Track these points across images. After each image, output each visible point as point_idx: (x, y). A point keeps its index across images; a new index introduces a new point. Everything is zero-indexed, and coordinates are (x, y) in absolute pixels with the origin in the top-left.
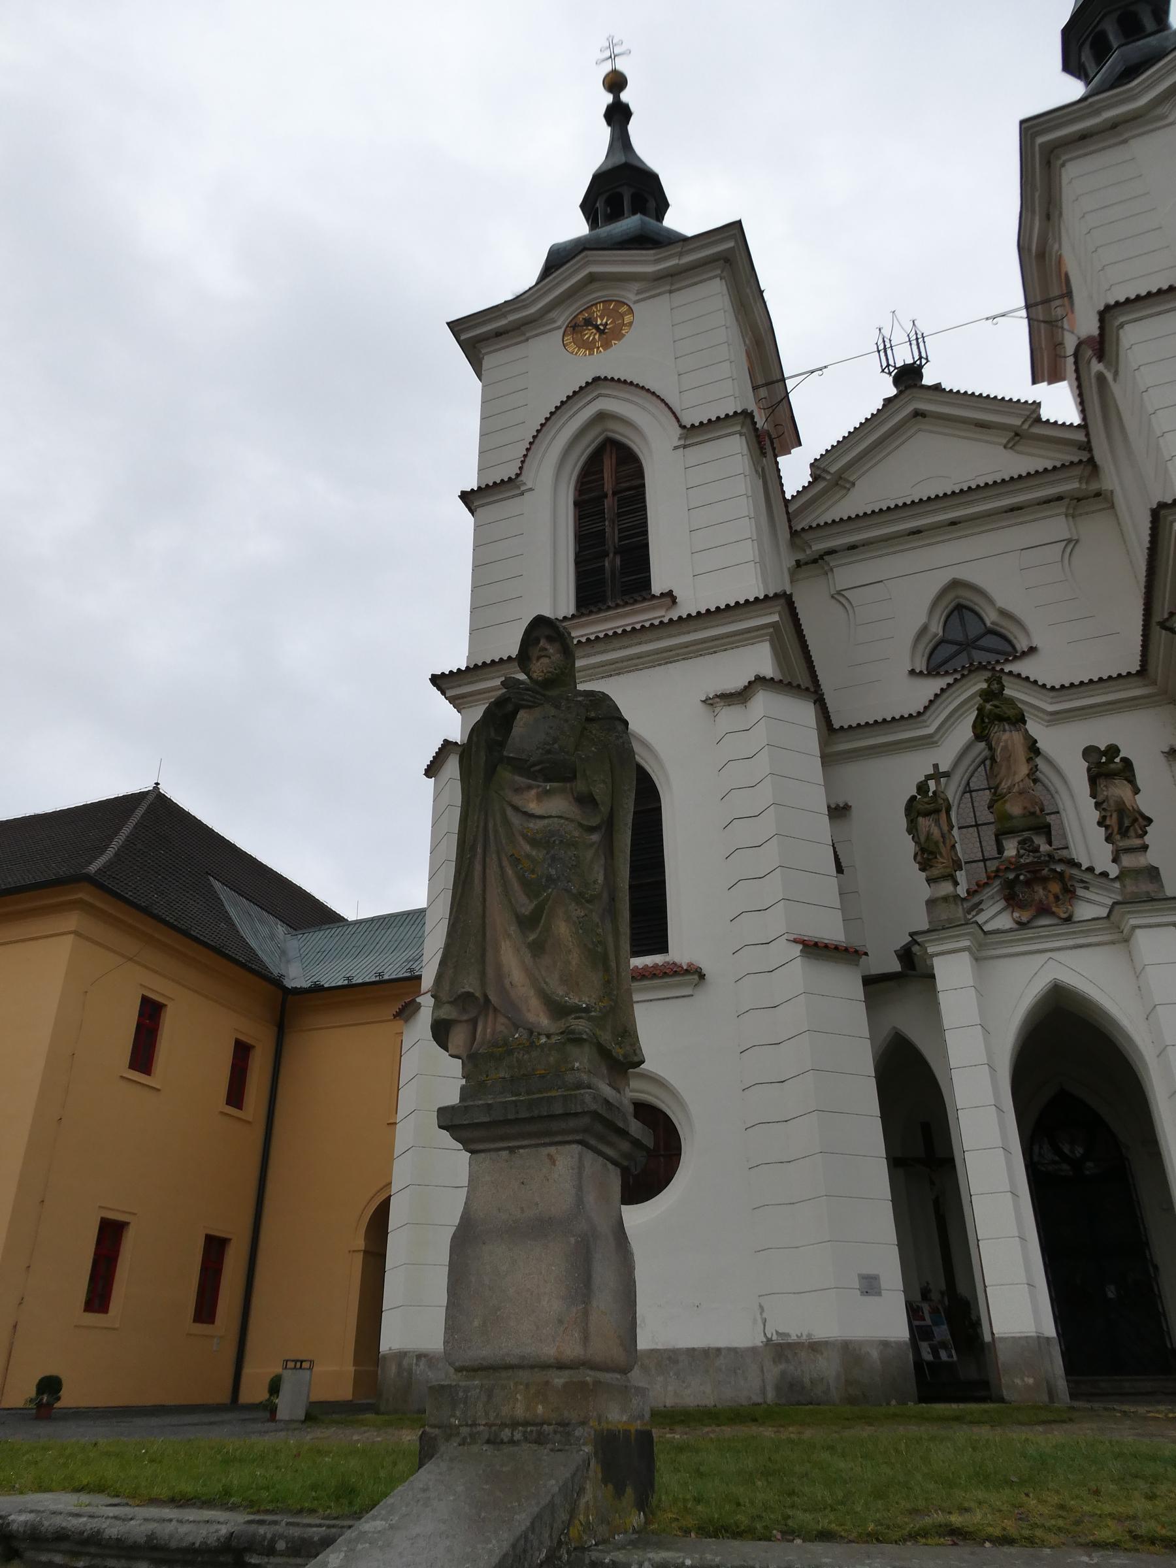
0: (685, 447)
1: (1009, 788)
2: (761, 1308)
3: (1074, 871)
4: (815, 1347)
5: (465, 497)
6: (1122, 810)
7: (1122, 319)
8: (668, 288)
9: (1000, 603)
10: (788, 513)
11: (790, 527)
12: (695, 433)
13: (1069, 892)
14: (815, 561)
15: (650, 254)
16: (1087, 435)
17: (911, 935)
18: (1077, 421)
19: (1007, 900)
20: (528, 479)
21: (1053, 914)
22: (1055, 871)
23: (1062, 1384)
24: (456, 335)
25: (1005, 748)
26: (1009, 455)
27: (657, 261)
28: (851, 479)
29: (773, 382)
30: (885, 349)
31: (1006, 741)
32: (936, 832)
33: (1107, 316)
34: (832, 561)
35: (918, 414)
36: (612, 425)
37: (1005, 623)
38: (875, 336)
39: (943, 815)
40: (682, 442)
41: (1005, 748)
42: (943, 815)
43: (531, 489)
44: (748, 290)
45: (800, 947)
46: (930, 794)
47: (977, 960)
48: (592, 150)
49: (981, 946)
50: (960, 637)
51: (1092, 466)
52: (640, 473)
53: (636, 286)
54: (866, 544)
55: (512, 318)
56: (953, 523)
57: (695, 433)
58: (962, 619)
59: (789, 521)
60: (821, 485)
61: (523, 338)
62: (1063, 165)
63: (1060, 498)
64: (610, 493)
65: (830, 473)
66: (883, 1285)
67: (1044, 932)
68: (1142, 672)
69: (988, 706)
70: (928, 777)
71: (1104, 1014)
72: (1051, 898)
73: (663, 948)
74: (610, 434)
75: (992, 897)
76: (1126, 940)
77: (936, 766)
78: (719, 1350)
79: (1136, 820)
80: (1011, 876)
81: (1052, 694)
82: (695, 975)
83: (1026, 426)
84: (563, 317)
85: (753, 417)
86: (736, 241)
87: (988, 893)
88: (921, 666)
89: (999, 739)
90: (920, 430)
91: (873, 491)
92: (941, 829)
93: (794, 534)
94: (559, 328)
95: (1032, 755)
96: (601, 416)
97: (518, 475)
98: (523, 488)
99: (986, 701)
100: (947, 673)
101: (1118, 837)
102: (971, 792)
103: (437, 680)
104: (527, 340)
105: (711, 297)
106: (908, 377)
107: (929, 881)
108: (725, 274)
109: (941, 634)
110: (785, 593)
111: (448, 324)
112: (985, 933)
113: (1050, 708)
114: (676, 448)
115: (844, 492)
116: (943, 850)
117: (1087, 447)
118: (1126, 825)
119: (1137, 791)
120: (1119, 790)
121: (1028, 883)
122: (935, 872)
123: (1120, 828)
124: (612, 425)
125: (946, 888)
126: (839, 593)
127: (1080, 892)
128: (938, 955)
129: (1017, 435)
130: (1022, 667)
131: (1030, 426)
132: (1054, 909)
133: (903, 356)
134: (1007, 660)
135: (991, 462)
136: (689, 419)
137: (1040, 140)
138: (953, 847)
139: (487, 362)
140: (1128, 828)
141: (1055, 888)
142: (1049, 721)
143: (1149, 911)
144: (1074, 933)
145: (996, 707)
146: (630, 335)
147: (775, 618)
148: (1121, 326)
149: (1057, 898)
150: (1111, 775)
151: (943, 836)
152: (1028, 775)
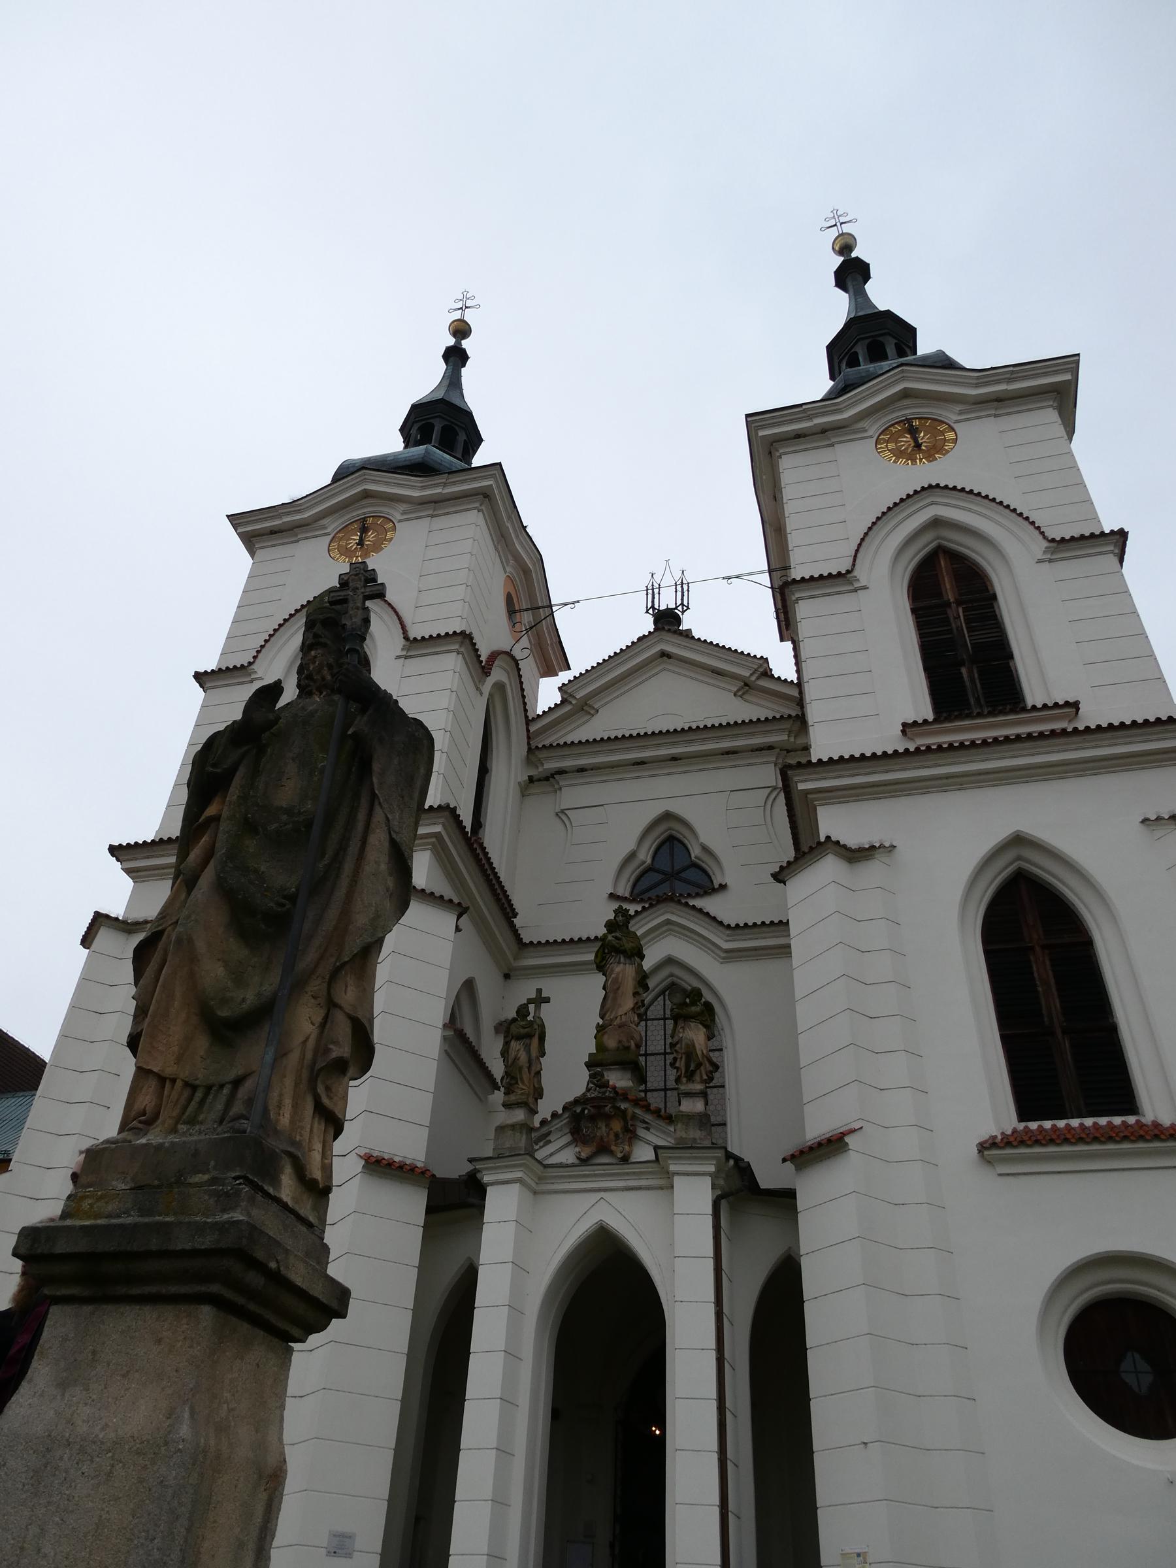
0: (406, 657)
1: (611, 1020)
5: (198, 676)
6: (690, 1053)
7: (797, 595)
8: (430, 512)
9: (703, 839)
10: (528, 731)
11: (529, 744)
12: (416, 645)
13: (631, 1135)
14: (547, 779)
15: (417, 481)
16: (801, 693)
17: (471, 1160)
18: (792, 676)
19: (572, 1134)
21: (612, 1153)
22: (619, 1108)
24: (235, 527)
25: (616, 980)
26: (738, 702)
27: (423, 488)
29: (531, 609)
30: (652, 591)
31: (618, 974)
32: (523, 1056)
33: (787, 591)
34: (562, 780)
35: (664, 654)
37: (705, 858)
39: (535, 1042)
40: (404, 653)
41: (616, 980)
42: (535, 1042)
44: (509, 525)
45: (363, 1162)
46: (530, 1018)
47: (535, 1193)
48: (426, 380)
49: (541, 1179)
50: (668, 869)
53: (403, 507)
54: (595, 768)
55: (285, 519)
56: (674, 759)
59: (529, 738)
60: (567, 708)
63: (770, 748)
65: (579, 700)
66: (357, 1546)
67: (599, 1170)
69: (610, 937)
70: (530, 1001)
72: (612, 1137)
75: (560, 1129)
77: (539, 991)
79: (699, 1065)
80: (578, 1110)
81: (728, 932)
83: (753, 678)
84: (333, 525)
85: (472, 639)
86: (496, 481)
87: (557, 1124)
89: (612, 971)
90: (664, 669)
91: (610, 721)
92: (529, 1052)
93: (530, 750)
94: (329, 534)
95: (641, 990)
97: (250, 664)
99: (610, 932)
100: (642, 901)
101: (684, 1080)
102: (646, 1020)
104: (298, 541)
105: (468, 529)
106: (667, 620)
108: (483, 508)
109: (649, 861)
110: (448, 805)
112: (546, 1166)
113: (725, 946)
114: (398, 657)
115: (588, 717)
116: (526, 1076)
122: (513, 1098)
123: (686, 1071)
125: (519, 1115)
126: (563, 811)
127: (641, 1132)
128: (492, 1184)
129: (746, 685)
130: (708, 904)
131: (758, 678)
132: (613, 1148)
133: (667, 601)
134: (698, 895)
135: (717, 705)
136: (415, 632)
137: (761, 433)
138: (538, 1073)
139: (259, 553)
140: (693, 1072)
141: (617, 1126)
142: (724, 958)
143: (689, 1158)
144: (628, 1174)
145: (616, 938)
146: (388, 549)
147: (438, 829)
148: (797, 599)
149: (617, 1135)
150: (688, 1018)
151: (530, 1061)
152: (633, 1009)
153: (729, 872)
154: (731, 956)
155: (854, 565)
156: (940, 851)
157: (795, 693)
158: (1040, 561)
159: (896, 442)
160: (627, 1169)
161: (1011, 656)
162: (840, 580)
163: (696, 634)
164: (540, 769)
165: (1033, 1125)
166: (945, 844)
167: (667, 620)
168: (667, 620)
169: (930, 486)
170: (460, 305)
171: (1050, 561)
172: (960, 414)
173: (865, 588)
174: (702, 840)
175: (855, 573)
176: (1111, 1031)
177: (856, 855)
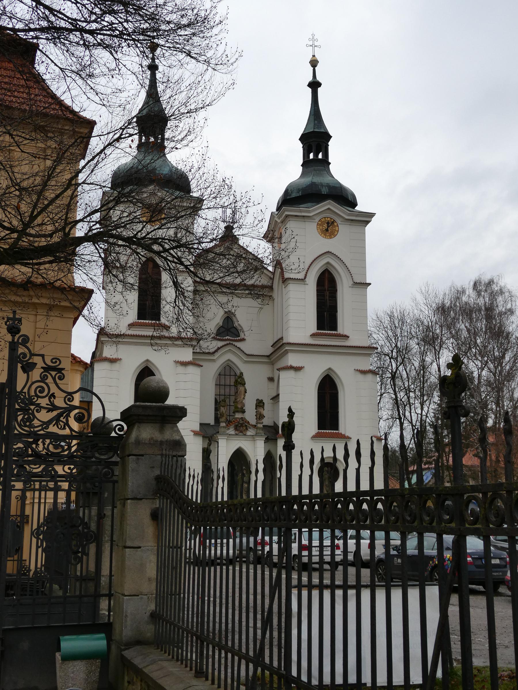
13: (247, 429)
32: (224, 411)
51: (271, 288)
58: (228, 321)
71: (246, 453)
117: (272, 279)
118: (260, 417)
120: (261, 410)
141: (245, 428)
150: (260, 406)
154: (246, 362)
155: (306, 275)
157: (272, 276)
162: (303, 280)
165: (320, 431)
166: (315, 368)
168: (229, 229)
169: (329, 252)
172: (342, 221)
175: (306, 280)
176: (337, 413)
177: (298, 369)
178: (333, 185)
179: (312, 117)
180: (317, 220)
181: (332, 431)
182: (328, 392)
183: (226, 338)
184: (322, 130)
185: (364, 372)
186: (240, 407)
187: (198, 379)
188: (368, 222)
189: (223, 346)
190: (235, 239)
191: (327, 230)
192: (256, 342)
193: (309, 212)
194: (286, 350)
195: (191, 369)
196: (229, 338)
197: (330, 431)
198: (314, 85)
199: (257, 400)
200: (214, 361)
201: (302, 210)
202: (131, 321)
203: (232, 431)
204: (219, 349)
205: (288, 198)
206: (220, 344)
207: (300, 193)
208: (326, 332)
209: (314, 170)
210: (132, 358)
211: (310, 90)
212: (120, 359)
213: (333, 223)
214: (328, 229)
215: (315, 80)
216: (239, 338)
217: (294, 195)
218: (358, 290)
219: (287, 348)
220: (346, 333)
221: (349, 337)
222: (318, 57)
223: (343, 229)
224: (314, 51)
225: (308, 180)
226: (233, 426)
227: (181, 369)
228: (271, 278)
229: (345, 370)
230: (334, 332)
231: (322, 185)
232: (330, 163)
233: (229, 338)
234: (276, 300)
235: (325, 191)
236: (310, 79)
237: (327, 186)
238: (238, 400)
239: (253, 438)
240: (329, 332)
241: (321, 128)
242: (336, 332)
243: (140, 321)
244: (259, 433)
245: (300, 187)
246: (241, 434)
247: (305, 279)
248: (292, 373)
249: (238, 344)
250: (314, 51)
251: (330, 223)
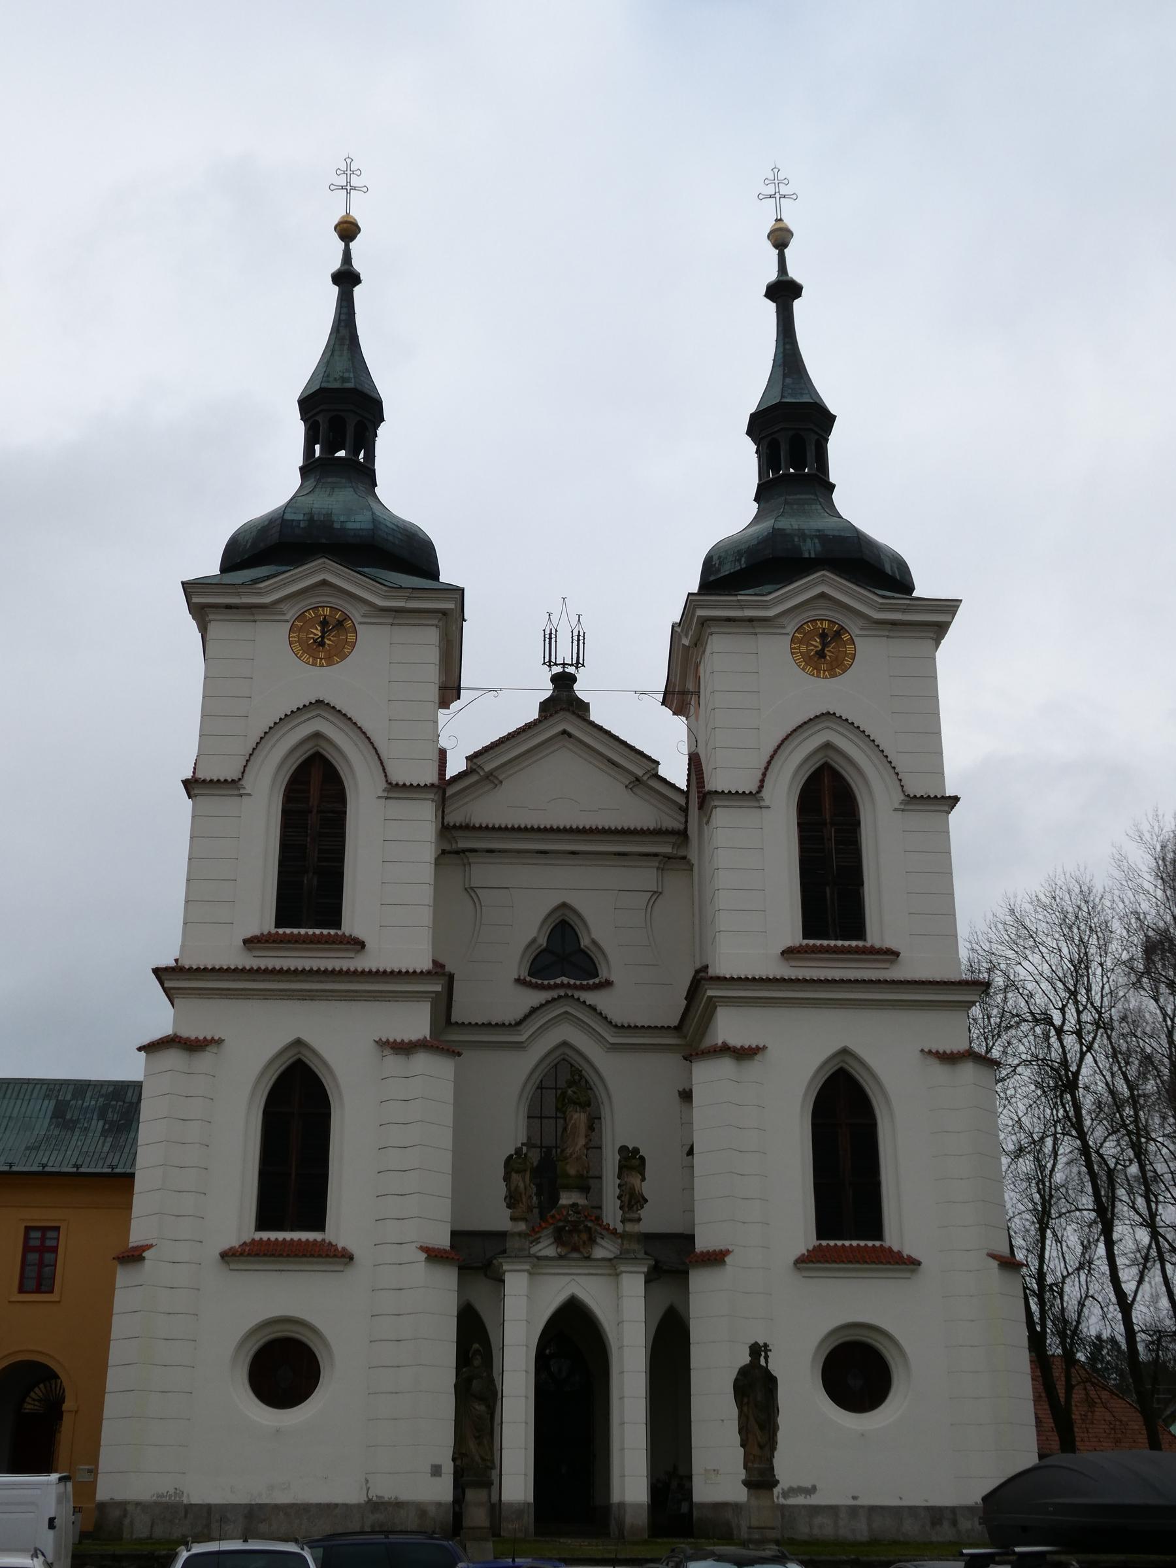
0: (386, 798)
2: (367, 1481)
3: (598, 1228)
4: (399, 1505)
8: (390, 621)
12: (396, 790)
13: (592, 1241)
14: (457, 852)
20: (248, 783)
23: (532, 1528)
27: (387, 597)
28: (501, 778)
30: (550, 638)
32: (521, 1185)
34: (472, 858)
35: (564, 732)
36: (324, 744)
37: (593, 948)
38: (542, 623)
43: (249, 795)
51: (682, 835)
52: (341, 797)
53: (365, 609)
54: (500, 851)
56: (573, 853)
57: (396, 790)
61: (251, 618)
62: (711, 634)
63: (656, 855)
64: (315, 810)
67: (572, 1263)
68: (678, 1028)
73: (320, 1226)
74: (321, 750)
76: (617, 1275)
78: (336, 1505)
80: (561, 1224)
82: (347, 1257)
88: (524, 974)
94: (287, 621)
96: (317, 735)
98: (242, 791)
103: (157, 972)
104: (255, 621)
107: (513, 1219)
111: (183, 583)
113: (612, 1040)
114: (379, 797)
115: (492, 786)
117: (685, 810)
118: (632, 1201)
119: (643, 1179)
120: (635, 1180)
121: (570, 1231)
124: (324, 744)
126: (472, 888)
127: (599, 1240)
133: (564, 652)
139: (214, 629)
141: (585, 1236)
147: (439, 988)
148: (716, 807)
149: (584, 1243)
150: (632, 1168)
153: (615, 966)
154: (615, 1048)
156: (797, 1049)
157: (682, 802)
158: (896, 810)
159: (808, 645)
160: (589, 1263)
161: (862, 884)
162: (752, 798)
163: (594, 716)
164: (454, 846)
165: (824, 1243)
167: (564, 681)
168: (564, 681)
169: (828, 715)
170: (342, 181)
171: (903, 810)
173: (768, 807)
174: (593, 936)
175: (763, 794)
176: (877, 1185)
178: (837, 533)
179: (780, 371)
180: (791, 628)
181: (862, 1243)
182: (844, 1120)
183: (558, 981)
184: (806, 399)
185: (949, 1059)
186: (572, 1171)
187: (447, 1091)
188: (939, 630)
189: (548, 1002)
190: (580, 709)
191: (821, 654)
192: (638, 990)
193: (765, 606)
194: (711, 998)
195: (422, 1062)
196: (565, 980)
197: (855, 1243)
198: (784, 292)
199: (623, 1149)
200: (519, 1046)
201: (745, 604)
202: (253, 930)
203: (546, 1248)
204: (533, 1011)
205: (712, 578)
206: (537, 998)
207: (743, 560)
208: (832, 943)
209: (786, 503)
210: (254, 1039)
211: (772, 306)
212: (218, 1042)
213: (838, 634)
214: (825, 651)
215: (784, 278)
216: (597, 980)
217: (726, 570)
218: (919, 819)
219: (710, 993)
220: (890, 943)
221: (897, 954)
222: (790, 222)
223: (870, 651)
224: (778, 208)
225: (767, 525)
226: (545, 1232)
227: (393, 1063)
228: (681, 808)
229: (890, 1052)
230: (854, 943)
231: (803, 535)
232: (833, 487)
233: (565, 980)
234: (696, 868)
235: (810, 549)
236: (772, 275)
237: (816, 536)
238: (569, 1151)
239: (612, 1267)
240: (840, 943)
241: (802, 394)
242: (860, 944)
243: (281, 931)
244: (628, 1251)
245: (743, 547)
246: (575, 1255)
247: (758, 792)
248: (725, 1067)
249: (590, 997)
250: (778, 208)
251: (831, 634)
